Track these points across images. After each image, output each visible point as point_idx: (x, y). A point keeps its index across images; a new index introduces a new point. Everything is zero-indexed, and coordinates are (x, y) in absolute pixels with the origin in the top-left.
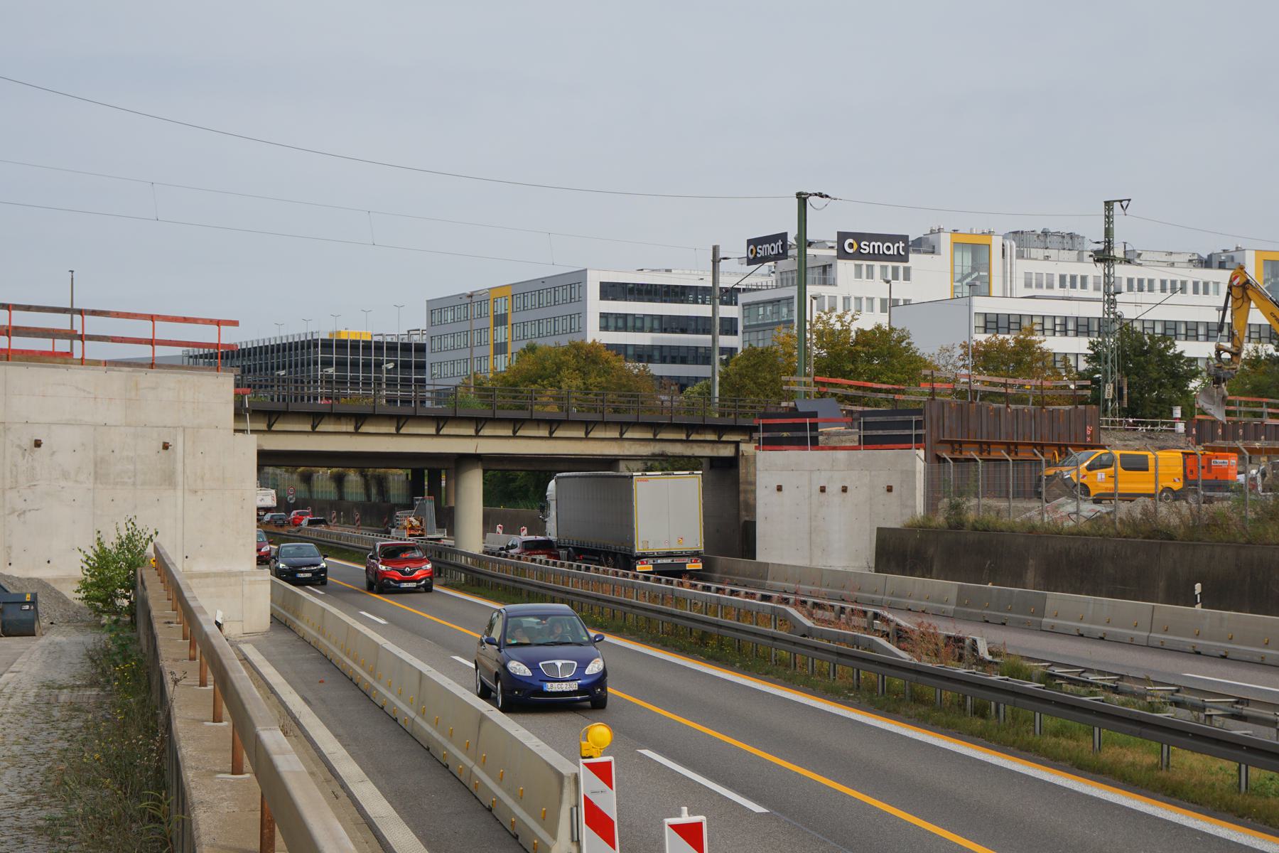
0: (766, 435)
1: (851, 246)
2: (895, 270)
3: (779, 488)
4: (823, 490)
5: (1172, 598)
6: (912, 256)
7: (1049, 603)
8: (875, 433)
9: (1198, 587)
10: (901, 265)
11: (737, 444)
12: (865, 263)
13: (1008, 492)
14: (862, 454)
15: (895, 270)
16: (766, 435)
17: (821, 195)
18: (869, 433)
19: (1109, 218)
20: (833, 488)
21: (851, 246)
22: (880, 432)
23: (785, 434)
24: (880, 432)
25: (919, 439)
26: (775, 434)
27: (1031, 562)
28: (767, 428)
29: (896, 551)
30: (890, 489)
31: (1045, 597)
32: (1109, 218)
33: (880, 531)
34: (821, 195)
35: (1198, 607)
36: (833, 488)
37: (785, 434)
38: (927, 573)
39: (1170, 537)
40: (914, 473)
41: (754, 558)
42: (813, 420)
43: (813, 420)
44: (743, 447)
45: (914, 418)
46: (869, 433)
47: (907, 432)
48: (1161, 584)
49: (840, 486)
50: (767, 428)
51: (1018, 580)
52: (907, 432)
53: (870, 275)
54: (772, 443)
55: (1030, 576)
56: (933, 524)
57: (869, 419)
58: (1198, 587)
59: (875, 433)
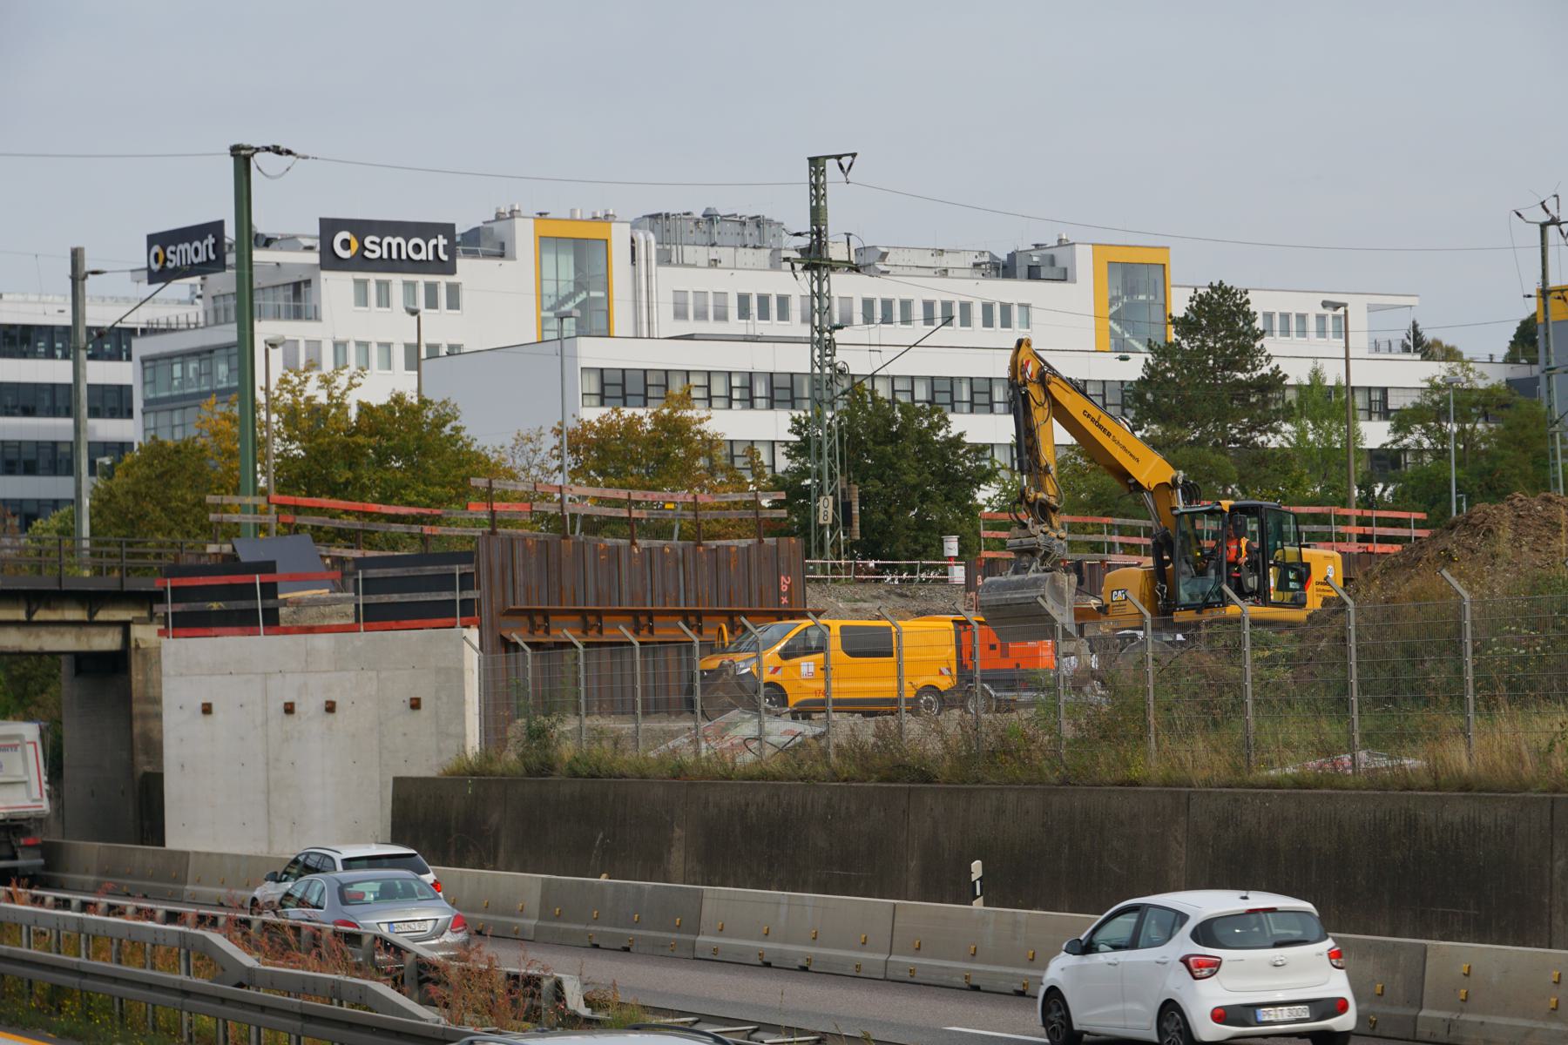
0: (180, 607)
1: (346, 244)
3: (207, 709)
4: (289, 709)
5: (930, 891)
7: (708, 908)
8: (385, 598)
9: (977, 867)
11: (125, 626)
12: (373, 277)
14: (362, 639)
16: (180, 607)
17: (277, 150)
18: (374, 599)
20: (310, 706)
21: (346, 244)
22: (395, 598)
23: (215, 606)
24: (395, 598)
27: (678, 832)
28: (180, 594)
29: (435, 821)
30: (415, 704)
31: (700, 896)
33: (398, 781)
34: (277, 150)
35: (978, 904)
36: (310, 706)
37: (215, 606)
38: (487, 860)
39: (927, 778)
40: (460, 673)
41: (161, 841)
42: (268, 578)
43: (268, 578)
44: (137, 632)
45: (458, 569)
46: (374, 599)
47: (445, 596)
48: (913, 864)
50: (180, 594)
51: (654, 866)
52: (445, 596)
53: (384, 300)
54: (190, 623)
55: (677, 858)
56: (498, 767)
57: (374, 573)
58: (977, 867)
59: (385, 598)
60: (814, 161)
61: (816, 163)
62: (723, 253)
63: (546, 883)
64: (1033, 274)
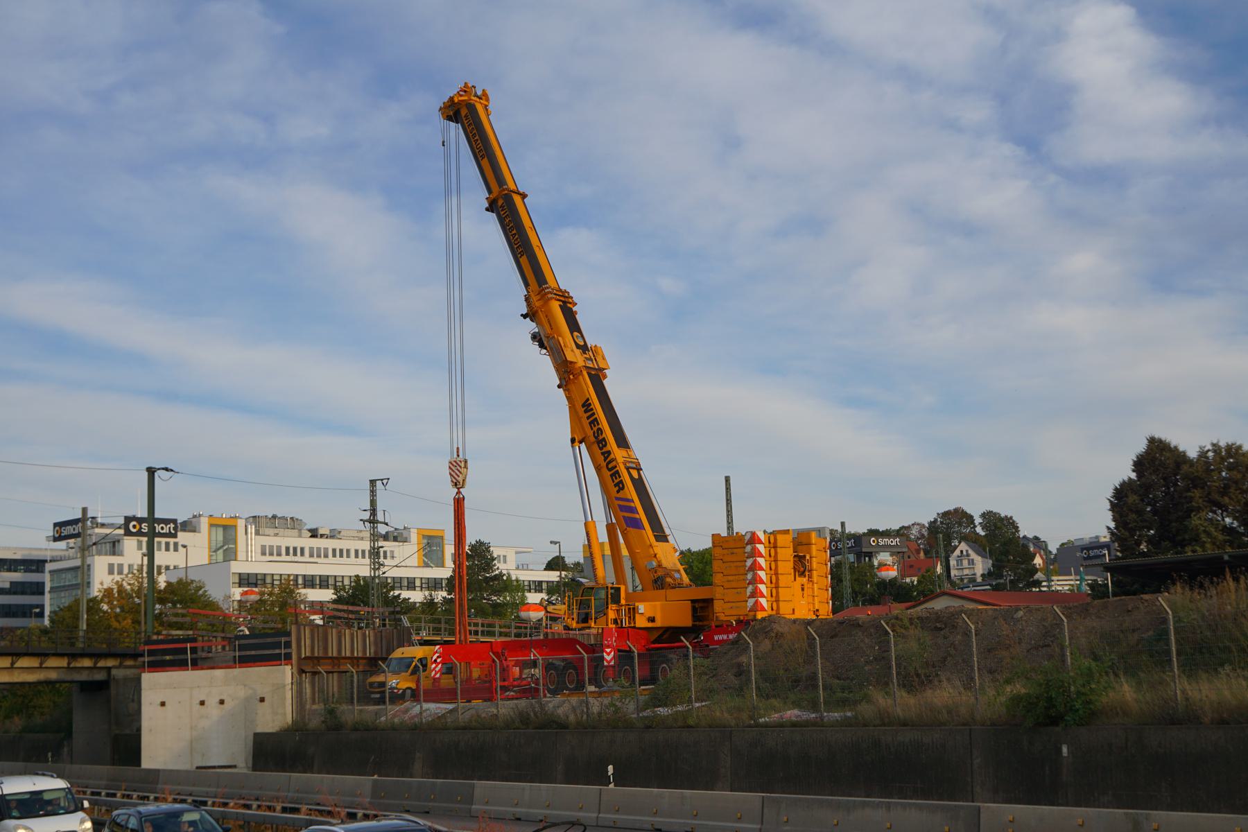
0: (151, 658)
1: (134, 527)
2: (167, 544)
3: (163, 704)
4: (202, 703)
5: (568, 781)
6: (179, 534)
7: (477, 792)
8: (248, 653)
9: (610, 768)
10: (172, 541)
11: (109, 669)
13: (352, 698)
14: (237, 672)
15: (167, 544)
16: (151, 658)
17: (167, 469)
18: (243, 653)
19: (373, 493)
20: (212, 702)
21: (134, 527)
22: (253, 653)
23: (168, 658)
24: (253, 653)
25: (288, 657)
26: (159, 658)
27: (418, 755)
28: (151, 653)
29: (270, 752)
31: (473, 786)
32: (373, 493)
33: (256, 735)
34: (167, 469)
35: (612, 786)
36: (212, 702)
37: (168, 658)
38: (308, 768)
41: (139, 764)
42: (194, 645)
43: (194, 645)
44: (114, 672)
45: (283, 640)
46: (243, 653)
47: (277, 651)
49: (217, 700)
50: (151, 653)
51: (405, 770)
52: (277, 651)
54: (157, 666)
55: (418, 766)
57: (243, 642)
58: (610, 768)
59: (248, 653)
60: (373, 482)
61: (373, 482)
62: (281, 531)
63: (375, 781)
64: (395, 539)
